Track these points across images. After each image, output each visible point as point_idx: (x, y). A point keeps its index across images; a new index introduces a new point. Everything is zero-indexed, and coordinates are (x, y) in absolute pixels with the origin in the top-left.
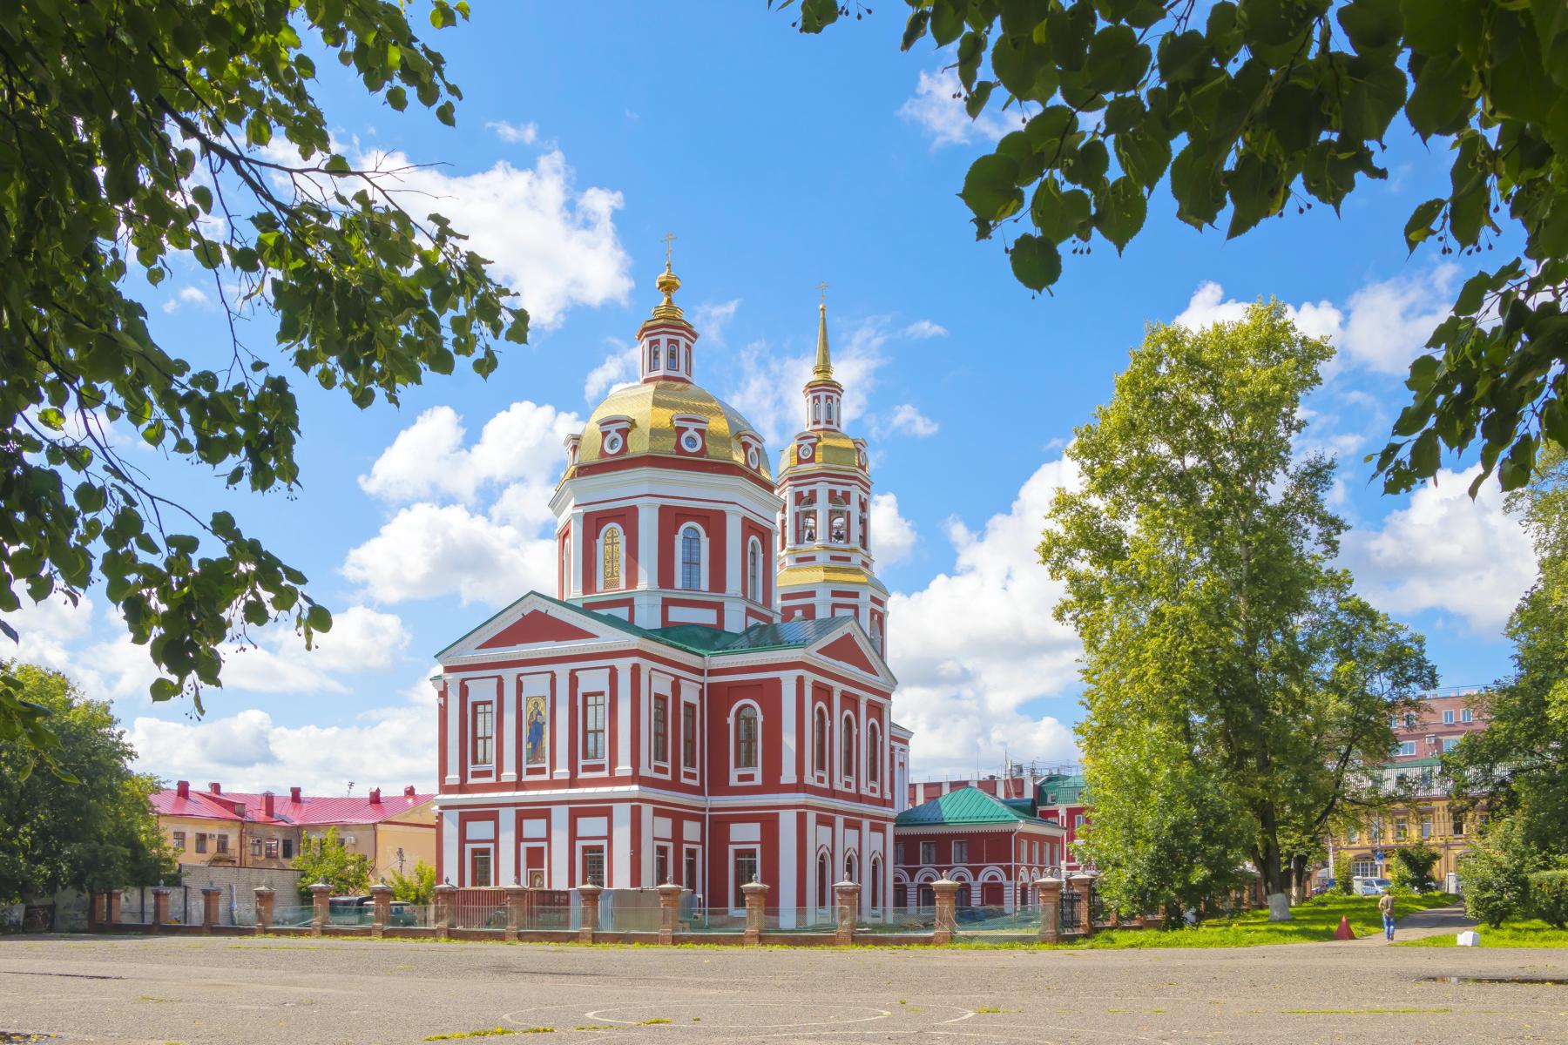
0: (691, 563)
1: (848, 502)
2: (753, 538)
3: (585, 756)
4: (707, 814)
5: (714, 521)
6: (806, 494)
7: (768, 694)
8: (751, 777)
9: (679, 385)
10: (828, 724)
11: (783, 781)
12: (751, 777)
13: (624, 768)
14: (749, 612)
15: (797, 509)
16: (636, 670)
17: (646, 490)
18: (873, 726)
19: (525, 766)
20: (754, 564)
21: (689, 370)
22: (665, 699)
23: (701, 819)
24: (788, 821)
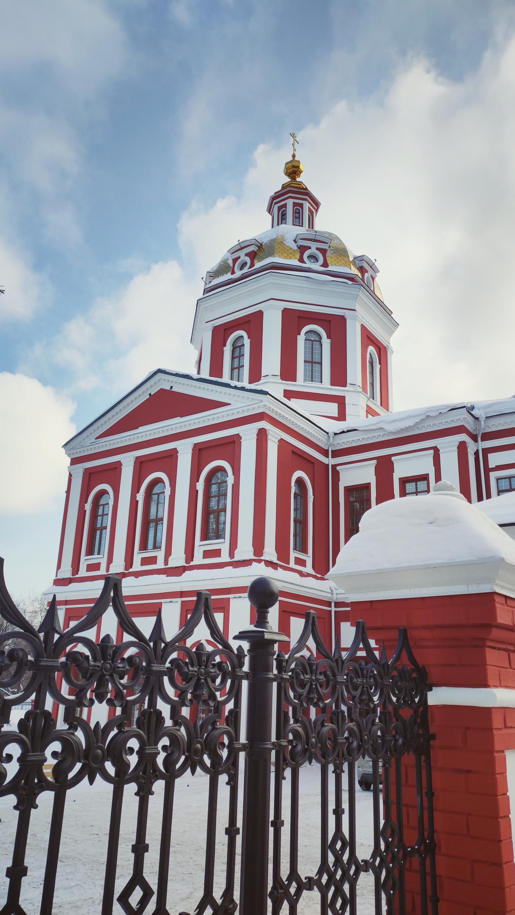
0: (313, 362)
4: (333, 609)
20: (372, 373)
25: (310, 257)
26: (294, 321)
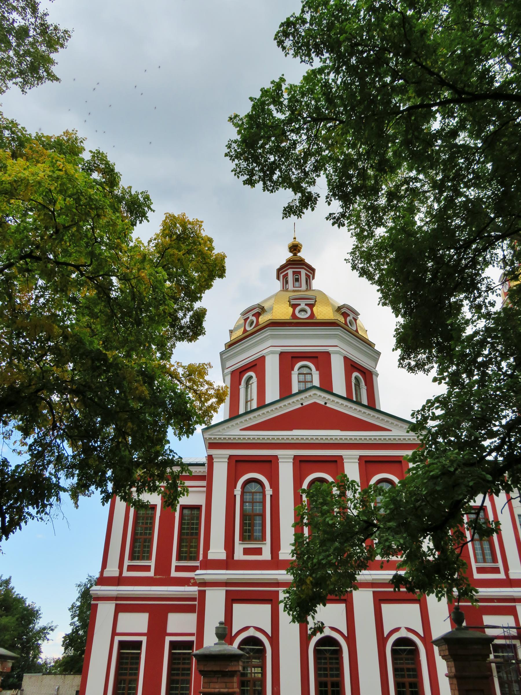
2: (355, 374)
5: (321, 360)
25: (300, 311)
26: (288, 360)
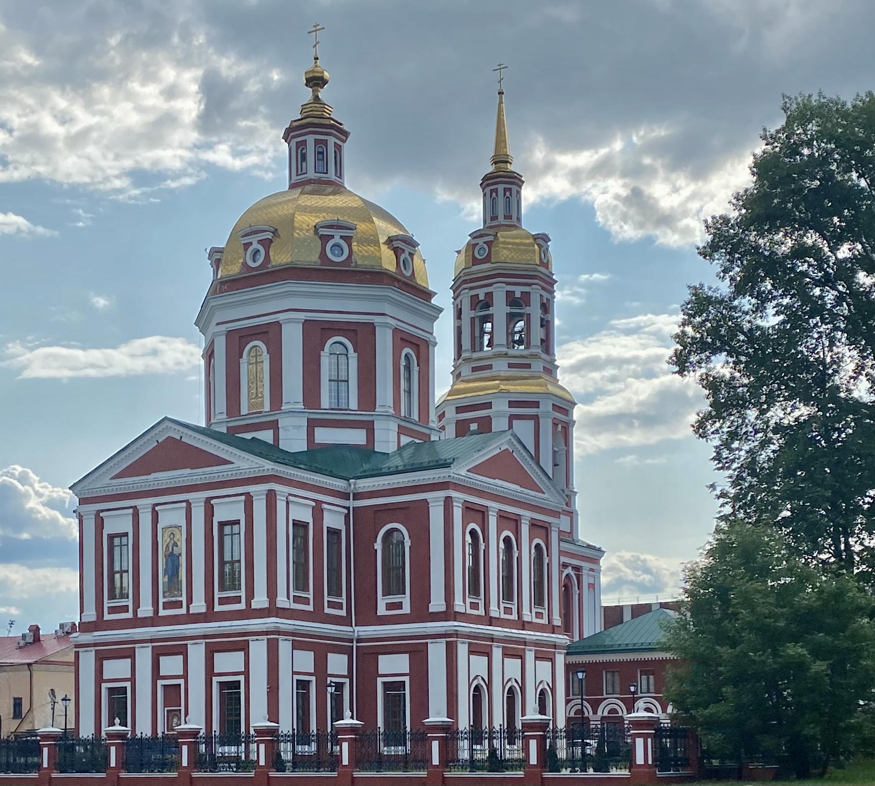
1: (528, 304)
2: (406, 350)
3: (222, 588)
5: (361, 335)
6: (482, 297)
7: (416, 516)
8: (399, 606)
9: (330, 189)
10: (482, 547)
11: (432, 609)
12: (399, 606)
13: (260, 600)
14: (402, 430)
15: (473, 314)
16: (271, 497)
17: (291, 307)
18: (538, 546)
19: (161, 600)
20: (409, 379)
21: (339, 173)
22: (305, 525)
23: (348, 651)
24: (437, 653)
